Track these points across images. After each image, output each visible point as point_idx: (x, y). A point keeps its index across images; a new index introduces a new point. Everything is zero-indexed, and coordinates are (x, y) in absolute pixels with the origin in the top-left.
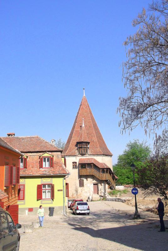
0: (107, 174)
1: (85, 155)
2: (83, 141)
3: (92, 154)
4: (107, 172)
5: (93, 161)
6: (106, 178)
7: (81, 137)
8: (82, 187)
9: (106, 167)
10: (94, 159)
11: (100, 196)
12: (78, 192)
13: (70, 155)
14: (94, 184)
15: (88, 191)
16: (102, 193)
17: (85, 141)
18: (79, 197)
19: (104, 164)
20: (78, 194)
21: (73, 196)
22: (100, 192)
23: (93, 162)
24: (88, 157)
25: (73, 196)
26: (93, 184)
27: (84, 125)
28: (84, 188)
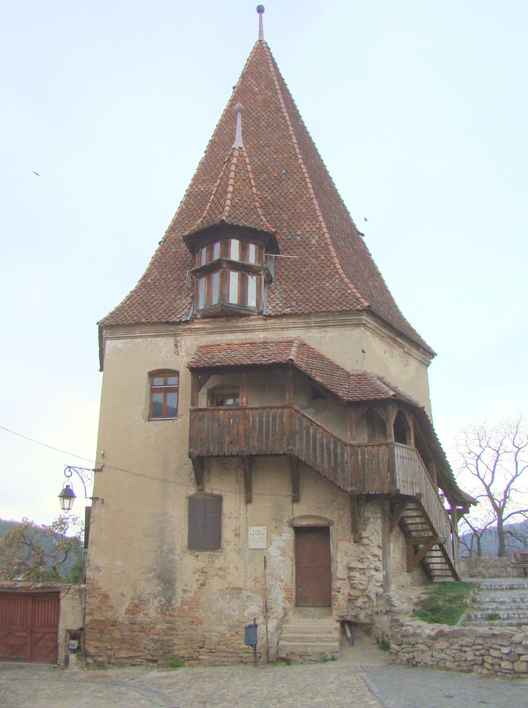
0: (400, 451)
1: (242, 323)
2: (224, 218)
3: (288, 310)
4: (401, 438)
5: (294, 349)
6: (393, 482)
7: (218, 205)
8: (204, 556)
9: (392, 393)
10: (303, 345)
11: (344, 623)
12: (179, 587)
13: (139, 324)
14: (299, 531)
15: (250, 584)
16: (360, 602)
17: (242, 223)
18: (179, 622)
19: (380, 379)
20: (177, 603)
21: (140, 617)
22: (346, 590)
23: (292, 357)
24: (260, 336)
25: (140, 617)
26: (288, 535)
27: (244, 138)
28: (217, 564)
